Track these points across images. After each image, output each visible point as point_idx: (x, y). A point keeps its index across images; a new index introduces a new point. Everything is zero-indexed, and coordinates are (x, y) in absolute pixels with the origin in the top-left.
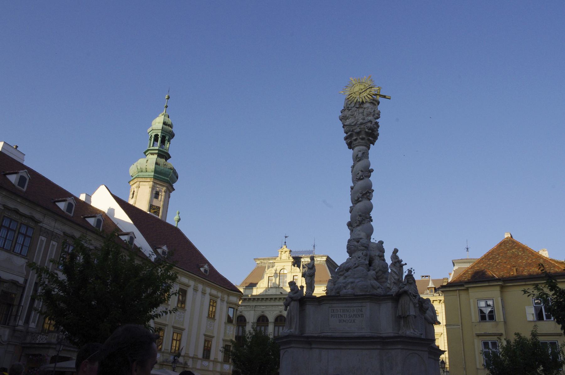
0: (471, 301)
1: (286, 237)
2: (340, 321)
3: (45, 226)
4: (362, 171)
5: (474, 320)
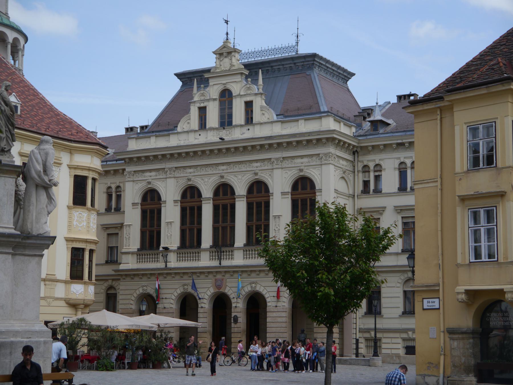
0: (457, 129)
5: (458, 169)
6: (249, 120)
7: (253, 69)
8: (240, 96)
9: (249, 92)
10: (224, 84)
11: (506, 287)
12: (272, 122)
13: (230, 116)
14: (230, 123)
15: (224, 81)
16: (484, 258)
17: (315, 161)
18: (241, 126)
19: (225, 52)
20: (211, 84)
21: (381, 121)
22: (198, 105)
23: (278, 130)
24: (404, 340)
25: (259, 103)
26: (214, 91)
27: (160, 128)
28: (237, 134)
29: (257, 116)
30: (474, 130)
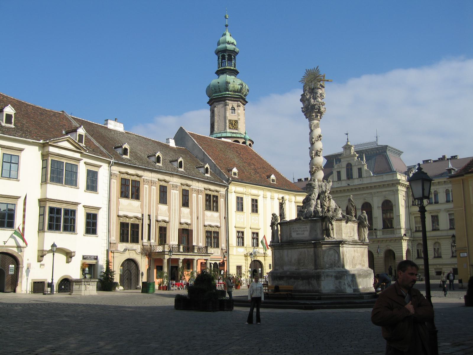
1: (347, 134)
2: (297, 234)
3: (145, 178)
6: (360, 176)
7: (360, 153)
10: (348, 161)
13: (352, 175)
14: (352, 178)
15: (348, 159)
19: (347, 147)
20: (342, 161)
22: (337, 170)
23: (375, 180)
24: (435, 269)
26: (344, 164)
28: (356, 182)
29: (364, 174)
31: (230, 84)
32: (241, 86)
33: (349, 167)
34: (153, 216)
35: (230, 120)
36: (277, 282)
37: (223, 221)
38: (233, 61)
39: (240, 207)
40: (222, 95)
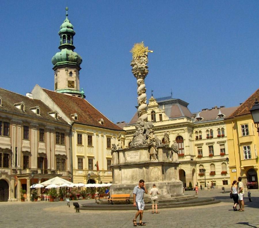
1: (152, 91)
2: (131, 158)
4: (140, 91)
6: (161, 120)
8: (158, 113)
9: (160, 112)
10: (152, 109)
11: (254, 165)
12: (168, 120)
15: (152, 109)
16: (248, 158)
17: (183, 131)
18: (159, 122)
21: (200, 118)
25: (163, 115)
27: (133, 123)
29: (163, 119)
30: (243, 127)
31: (69, 55)
32: (77, 57)
33: (153, 114)
34: (19, 148)
35: (69, 81)
36: (117, 192)
37: (68, 151)
38: (71, 40)
39: (80, 142)
40: (63, 63)
